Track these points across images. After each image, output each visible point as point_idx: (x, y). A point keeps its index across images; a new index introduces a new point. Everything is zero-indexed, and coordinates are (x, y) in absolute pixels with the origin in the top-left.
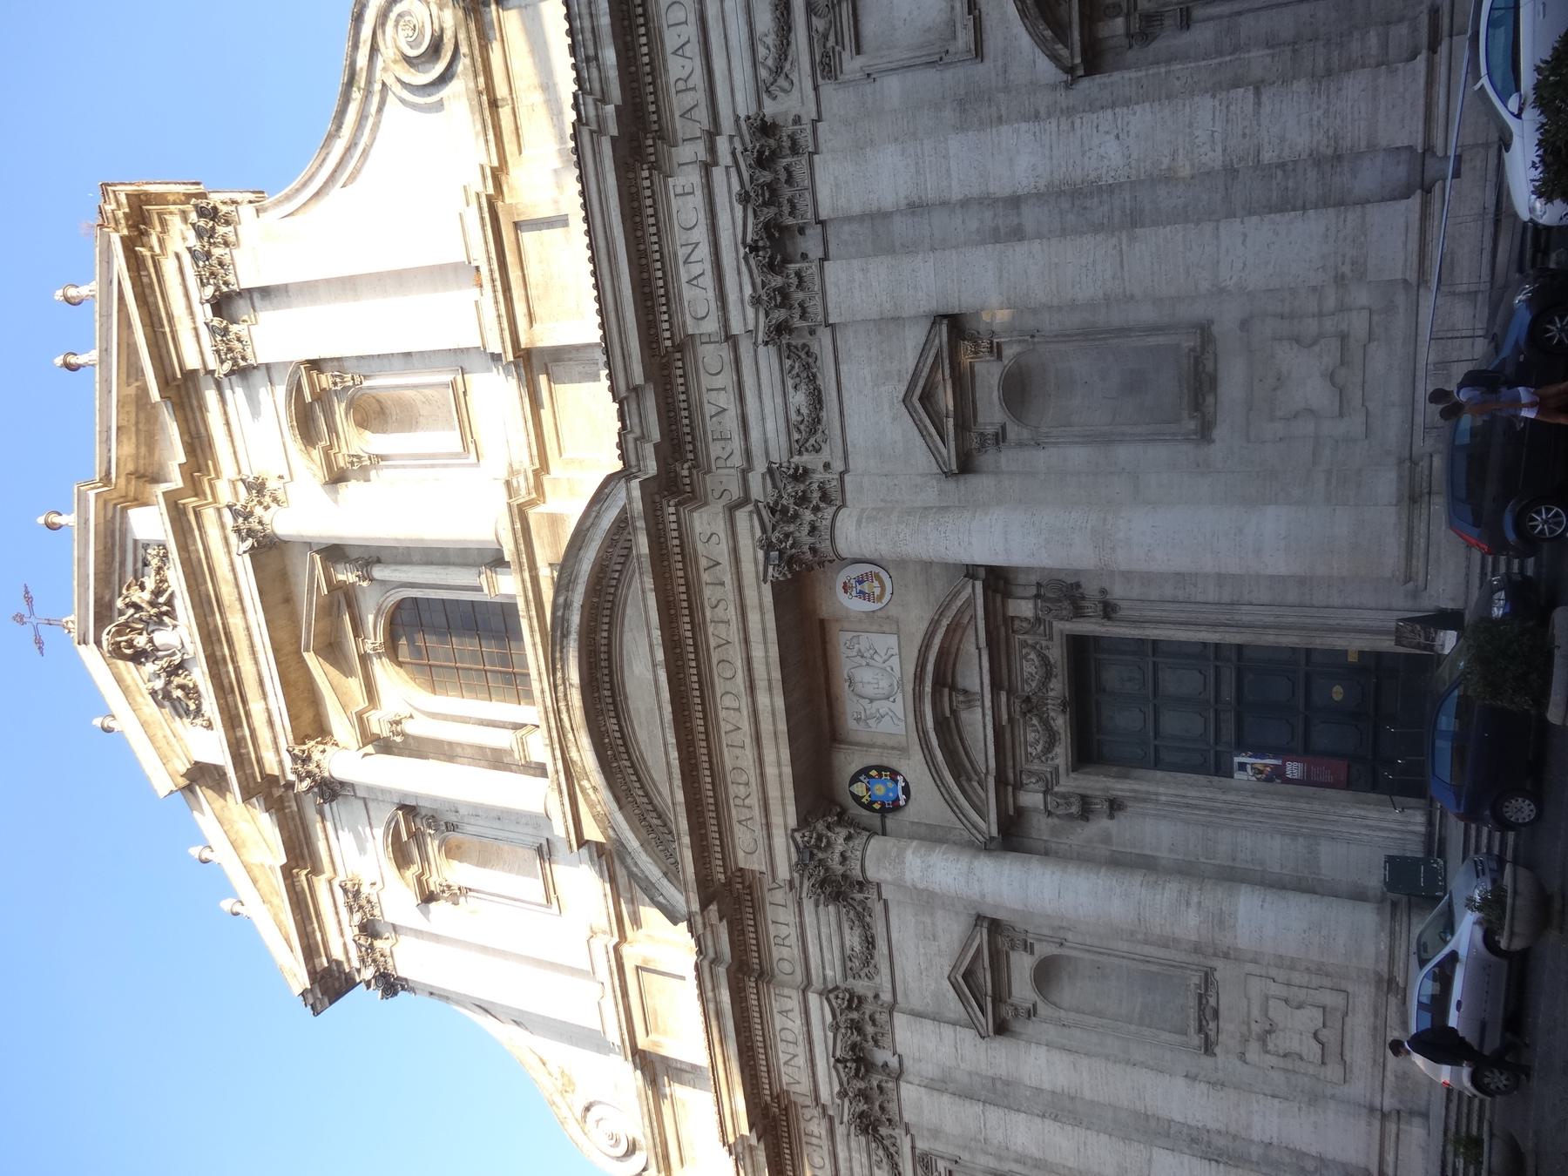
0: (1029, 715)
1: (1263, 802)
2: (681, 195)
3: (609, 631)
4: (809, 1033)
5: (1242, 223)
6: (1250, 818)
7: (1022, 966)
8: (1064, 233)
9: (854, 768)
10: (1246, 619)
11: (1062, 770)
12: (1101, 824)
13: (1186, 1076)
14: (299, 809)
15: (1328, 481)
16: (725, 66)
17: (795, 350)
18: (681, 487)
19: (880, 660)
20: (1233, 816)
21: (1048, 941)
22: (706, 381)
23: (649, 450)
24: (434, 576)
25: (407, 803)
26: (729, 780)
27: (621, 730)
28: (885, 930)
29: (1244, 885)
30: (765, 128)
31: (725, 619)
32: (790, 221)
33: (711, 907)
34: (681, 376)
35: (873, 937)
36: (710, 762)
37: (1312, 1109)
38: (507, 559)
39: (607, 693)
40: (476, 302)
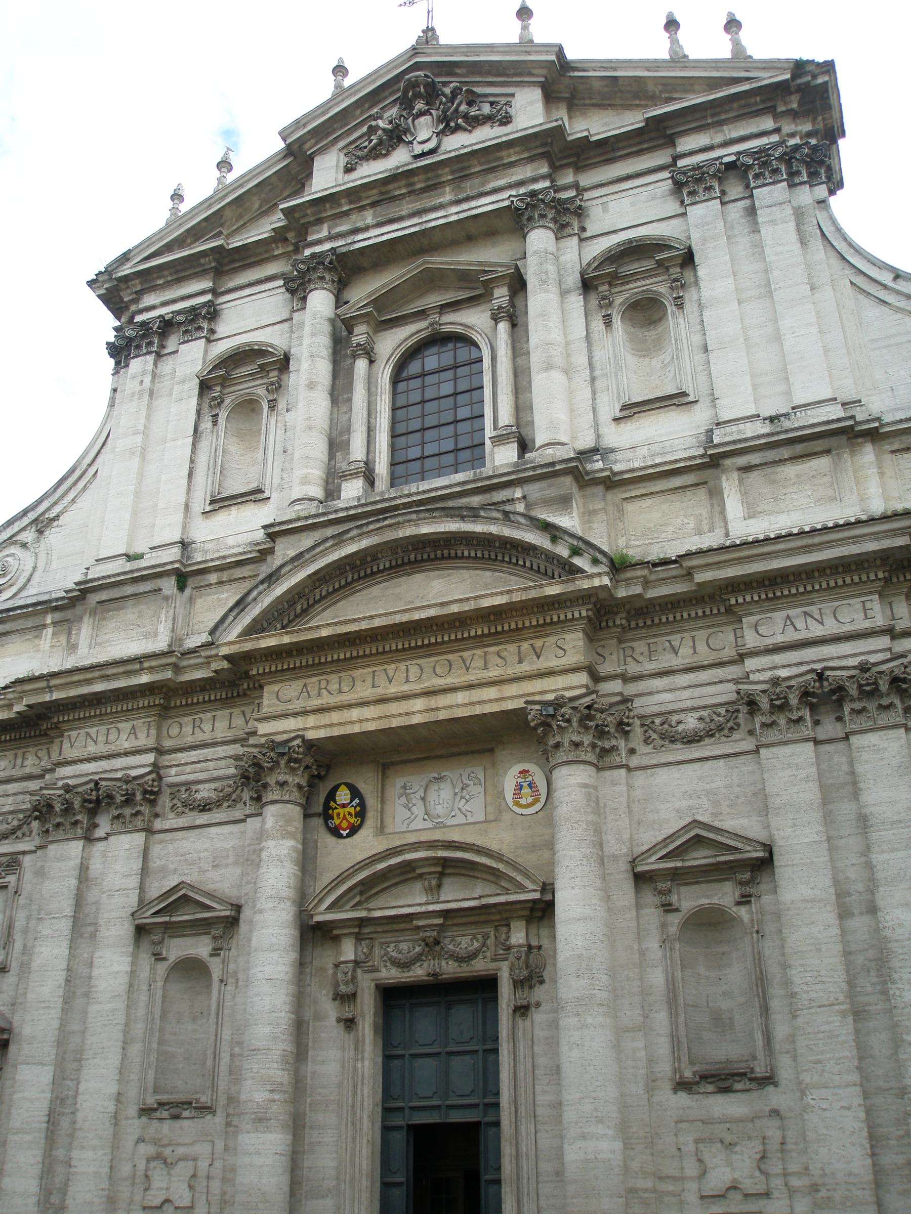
0: (423, 944)
1: (364, 1150)
2: (864, 607)
3: (469, 557)
5: (860, 1105)
6: (349, 1140)
8: (847, 954)
9: (362, 786)
10: (523, 1129)
11: (376, 975)
12: (331, 1011)
13: (119, 1094)
14: (275, 256)
15: (646, 1190)
17: (734, 716)
18: (605, 618)
19: (460, 806)
20: (349, 1124)
21: (223, 969)
22: (701, 635)
23: (637, 590)
24: (505, 382)
25: (291, 363)
26: (343, 674)
27: (379, 571)
28: (218, 821)
29: (290, 1137)
31: (489, 665)
32: (847, 709)
33: (225, 662)
34: (704, 612)
35: (210, 810)
36: (358, 657)
37: (104, 1199)
38: (527, 455)
39: (412, 557)
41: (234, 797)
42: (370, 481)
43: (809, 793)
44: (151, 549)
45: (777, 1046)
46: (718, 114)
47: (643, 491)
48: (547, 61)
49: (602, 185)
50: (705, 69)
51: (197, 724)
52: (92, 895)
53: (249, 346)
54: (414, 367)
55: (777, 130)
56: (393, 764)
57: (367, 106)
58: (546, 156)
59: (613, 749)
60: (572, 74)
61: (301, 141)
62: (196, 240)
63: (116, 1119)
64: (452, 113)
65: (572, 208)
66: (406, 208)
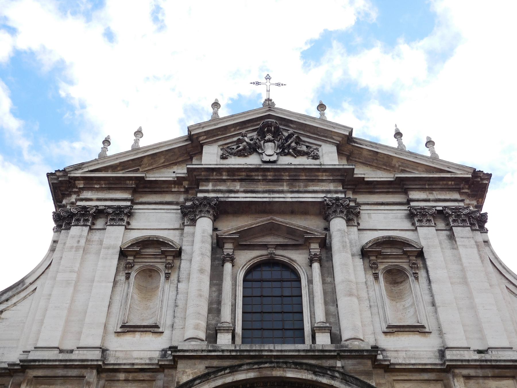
25: (183, 254)
40: (469, 348)
44: (78, 348)
46: (432, 185)
47: (406, 378)
48: (344, 134)
49: (368, 204)
50: (426, 161)
53: (157, 238)
54: (256, 275)
55: (462, 201)
58: (343, 182)
60: (354, 144)
61: (199, 135)
62: (122, 170)
64: (287, 146)
65: (354, 211)
66: (261, 187)
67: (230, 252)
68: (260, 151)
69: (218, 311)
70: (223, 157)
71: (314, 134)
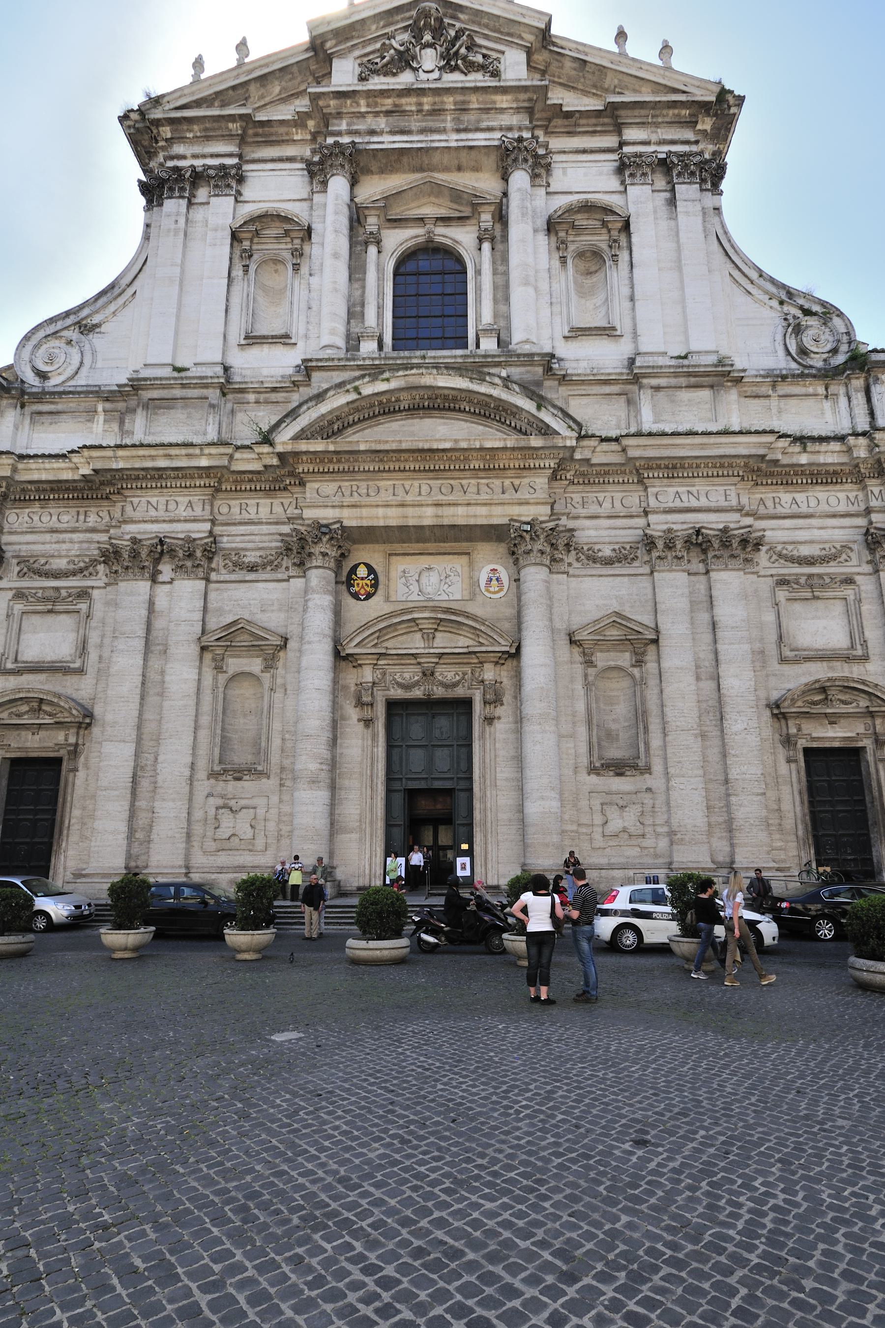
4: (179, 521)
7: (255, 665)
12: (353, 713)
15: (572, 831)
16: (787, 526)
22: (618, 496)
25: (313, 236)
30: (757, 545)
32: (710, 554)
41: (276, 563)
42: (381, 347)
43: (683, 604)
45: (652, 752)
46: (657, 116)
49: (564, 152)
50: (654, 74)
51: (244, 506)
52: (159, 624)
56: (396, 554)
57: (382, 23)
59: (562, 560)
60: (552, 48)
63: (191, 779)
65: (543, 162)
67: (374, 229)
68: (415, 65)
69: (362, 314)
70: (362, 79)
71: (495, 31)
